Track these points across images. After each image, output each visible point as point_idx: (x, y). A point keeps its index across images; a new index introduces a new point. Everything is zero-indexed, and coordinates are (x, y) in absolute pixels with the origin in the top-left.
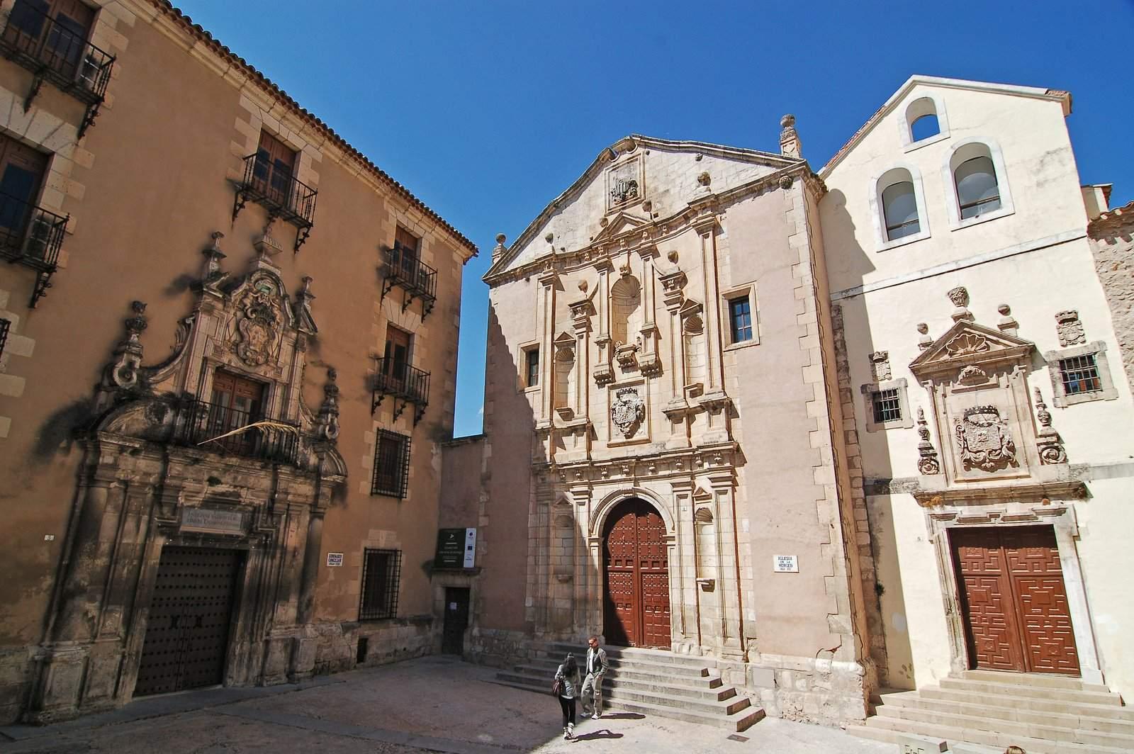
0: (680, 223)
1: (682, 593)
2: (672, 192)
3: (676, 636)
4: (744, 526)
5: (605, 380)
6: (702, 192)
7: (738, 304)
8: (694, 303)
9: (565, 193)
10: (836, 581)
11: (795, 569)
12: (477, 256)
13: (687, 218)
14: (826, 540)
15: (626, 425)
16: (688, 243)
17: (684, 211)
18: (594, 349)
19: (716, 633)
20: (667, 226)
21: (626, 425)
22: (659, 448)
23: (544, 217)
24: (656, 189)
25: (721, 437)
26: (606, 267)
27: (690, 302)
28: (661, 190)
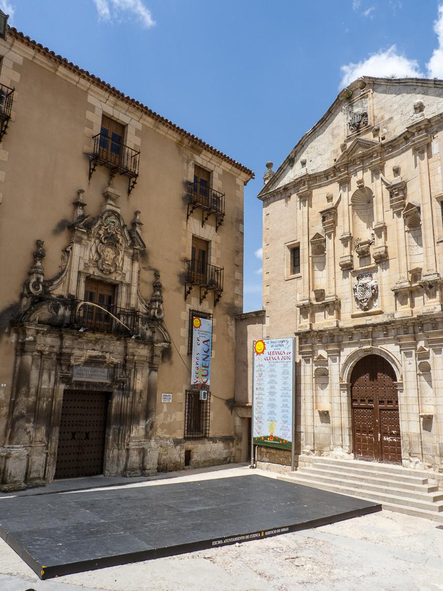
0: (402, 143)
1: (409, 425)
2: (395, 118)
3: (404, 455)
6: (418, 118)
9: (314, 127)
12: (254, 178)
13: (406, 139)
15: (365, 300)
17: (404, 133)
18: (339, 244)
20: (392, 147)
21: (365, 300)
22: (389, 317)
23: (300, 147)
25: (435, 308)
26: (344, 183)
27: (410, 205)
28: (387, 117)
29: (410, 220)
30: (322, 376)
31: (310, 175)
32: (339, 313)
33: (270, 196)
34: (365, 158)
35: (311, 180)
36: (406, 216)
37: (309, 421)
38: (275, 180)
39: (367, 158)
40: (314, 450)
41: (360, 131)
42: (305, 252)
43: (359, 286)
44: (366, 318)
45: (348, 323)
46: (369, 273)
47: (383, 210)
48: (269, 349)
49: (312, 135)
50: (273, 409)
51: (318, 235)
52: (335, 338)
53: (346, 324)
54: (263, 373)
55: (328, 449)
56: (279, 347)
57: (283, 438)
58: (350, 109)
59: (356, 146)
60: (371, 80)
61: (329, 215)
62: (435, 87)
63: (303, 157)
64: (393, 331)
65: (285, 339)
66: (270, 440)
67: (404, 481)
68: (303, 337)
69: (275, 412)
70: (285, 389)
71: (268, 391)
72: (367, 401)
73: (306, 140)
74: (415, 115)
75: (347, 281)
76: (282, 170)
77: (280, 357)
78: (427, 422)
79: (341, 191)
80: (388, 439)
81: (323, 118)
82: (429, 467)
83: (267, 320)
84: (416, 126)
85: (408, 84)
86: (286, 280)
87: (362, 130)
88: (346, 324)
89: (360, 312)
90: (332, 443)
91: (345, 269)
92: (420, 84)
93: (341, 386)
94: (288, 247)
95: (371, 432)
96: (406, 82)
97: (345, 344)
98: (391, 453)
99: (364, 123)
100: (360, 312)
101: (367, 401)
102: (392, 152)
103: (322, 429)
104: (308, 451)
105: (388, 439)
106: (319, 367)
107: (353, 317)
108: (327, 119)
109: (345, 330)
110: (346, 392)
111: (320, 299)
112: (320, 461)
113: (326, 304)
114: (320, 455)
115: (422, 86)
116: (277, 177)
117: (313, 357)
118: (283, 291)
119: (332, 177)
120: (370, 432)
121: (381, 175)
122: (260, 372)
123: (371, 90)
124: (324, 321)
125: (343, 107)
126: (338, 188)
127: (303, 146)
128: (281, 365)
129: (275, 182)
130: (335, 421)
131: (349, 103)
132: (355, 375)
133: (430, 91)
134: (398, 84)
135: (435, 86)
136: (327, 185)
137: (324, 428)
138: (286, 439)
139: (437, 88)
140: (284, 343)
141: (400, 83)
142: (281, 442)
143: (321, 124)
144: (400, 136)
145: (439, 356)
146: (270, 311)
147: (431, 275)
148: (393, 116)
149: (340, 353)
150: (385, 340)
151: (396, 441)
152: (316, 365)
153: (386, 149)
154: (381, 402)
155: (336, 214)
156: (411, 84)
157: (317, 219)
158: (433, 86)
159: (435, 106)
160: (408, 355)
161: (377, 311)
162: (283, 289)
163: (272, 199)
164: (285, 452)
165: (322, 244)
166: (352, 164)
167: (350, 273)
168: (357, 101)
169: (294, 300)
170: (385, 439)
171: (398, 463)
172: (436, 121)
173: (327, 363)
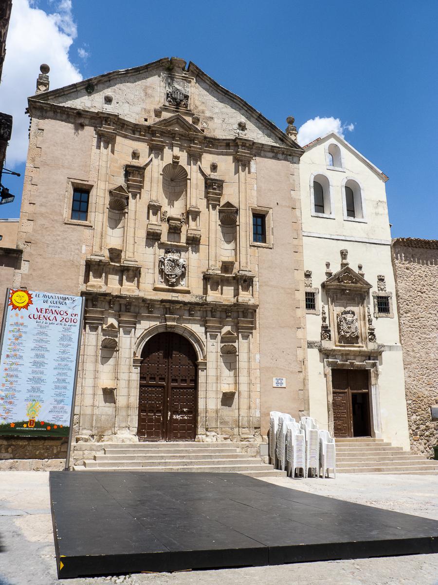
0: (221, 146)
1: (208, 401)
2: (216, 120)
3: (200, 430)
4: (257, 359)
5: (153, 237)
7: (260, 218)
8: (232, 206)
9: (128, 70)
10: (304, 393)
11: (284, 385)
14: (300, 370)
15: (173, 276)
16: (226, 164)
17: (229, 140)
19: (234, 426)
21: (173, 276)
22: (197, 298)
23: (106, 79)
24: (203, 112)
25: (250, 300)
26: (156, 150)
27: (228, 204)
28: (208, 114)
29: (223, 216)
30: (109, 348)
31: (119, 119)
32: (138, 282)
33: (49, 109)
34: (184, 138)
35: (116, 124)
36: (220, 212)
37: (88, 401)
38: (60, 95)
39: (185, 140)
40: (94, 435)
41: (179, 109)
42: (99, 200)
43: (168, 260)
44: (172, 293)
45: (150, 295)
46: (179, 250)
47: (196, 194)
48: (38, 303)
49: (122, 76)
50: (38, 385)
51: (120, 188)
52: (130, 309)
53: (148, 295)
54: (23, 335)
55: (110, 432)
56: (58, 305)
57: (53, 423)
58: (169, 81)
59: (174, 121)
60: (198, 71)
61: (134, 173)
62: (256, 119)
63: (108, 92)
64: (199, 312)
65: (69, 297)
66: (27, 427)
67: (219, 453)
68: (91, 299)
69: (42, 389)
70: (63, 359)
71: (32, 360)
72: (157, 378)
73: (116, 77)
74: (238, 131)
75: (150, 250)
76: (75, 90)
77: (59, 318)
78: (228, 399)
79: (152, 155)
80: (178, 417)
81: (138, 68)
82: (225, 439)
83: (25, 266)
84: (244, 141)
85: (235, 100)
86: (66, 224)
87: (181, 109)
88: (148, 295)
89: (164, 286)
90: (116, 425)
91: (151, 237)
92: (246, 109)
93: (135, 361)
94: (73, 183)
95: (159, 411)
96: (234, 98)
97: (143, 316)
98: (180, 430)
99: (184, 104)
100: (164, 286)
101: (157, 378)
102: (210, 147)
103: (105, 409)
104: (87, 437)
105: (178, 417)
106: (107, 337)
107: (155, 289)
108: (141, 72)
109: (149, 302)
110: (139, 368)
111: (116, 260)
112: (109, 446)
113: (125, 268)
114: (98, 441)
115: (246, 111)
116: (65, 93)
117: (101, 324)
118: (59, 235)
119: (140, 135)
120: (157, 411)
121: (199, 163)
122: (17, 334)
123: (195, 79)
124: (113, 285)
125: (162, 74)
126: (147, 150)
127: (110, 81)
128: (60, 328)
129: (59, 96)
130: (121, 400)
131: (169, 74)
132: (146, 352)
133: (252, 119)
134: (224, 94)
135: (258, 119)
136: (133, 140)
137: (107, 409)
138: (60, 423)
139: (258, 121)
140: (67, 301)
141: (226, 94)
142: (49, 428)
143: (134, 72)
144: (224, 140)
145: (245, 341)
146: (31, 255)
147: (246, 271)
148: (213, 117)
149: (135, 325)
150: (190, 319)
151: (186, 418)
152: (104, 335)
153: (206, 142)
154: (175, 380)
155: (143, 176)
156: (238, 102)
157: (118, 170)
158: (256, 117)
159: (255, 134)
160: (214, 337)
161: (185, 290)
162: (59, 233)
163: (51, 114)
164: (47, 441)
165: (123, 200)
166: (168, 135)
167: (156, 243)
168: (178, 78)
169: (77, 251)
170: (174, 417)
171: (187, 439)
172: (257, 147)
173: (116, 334)
